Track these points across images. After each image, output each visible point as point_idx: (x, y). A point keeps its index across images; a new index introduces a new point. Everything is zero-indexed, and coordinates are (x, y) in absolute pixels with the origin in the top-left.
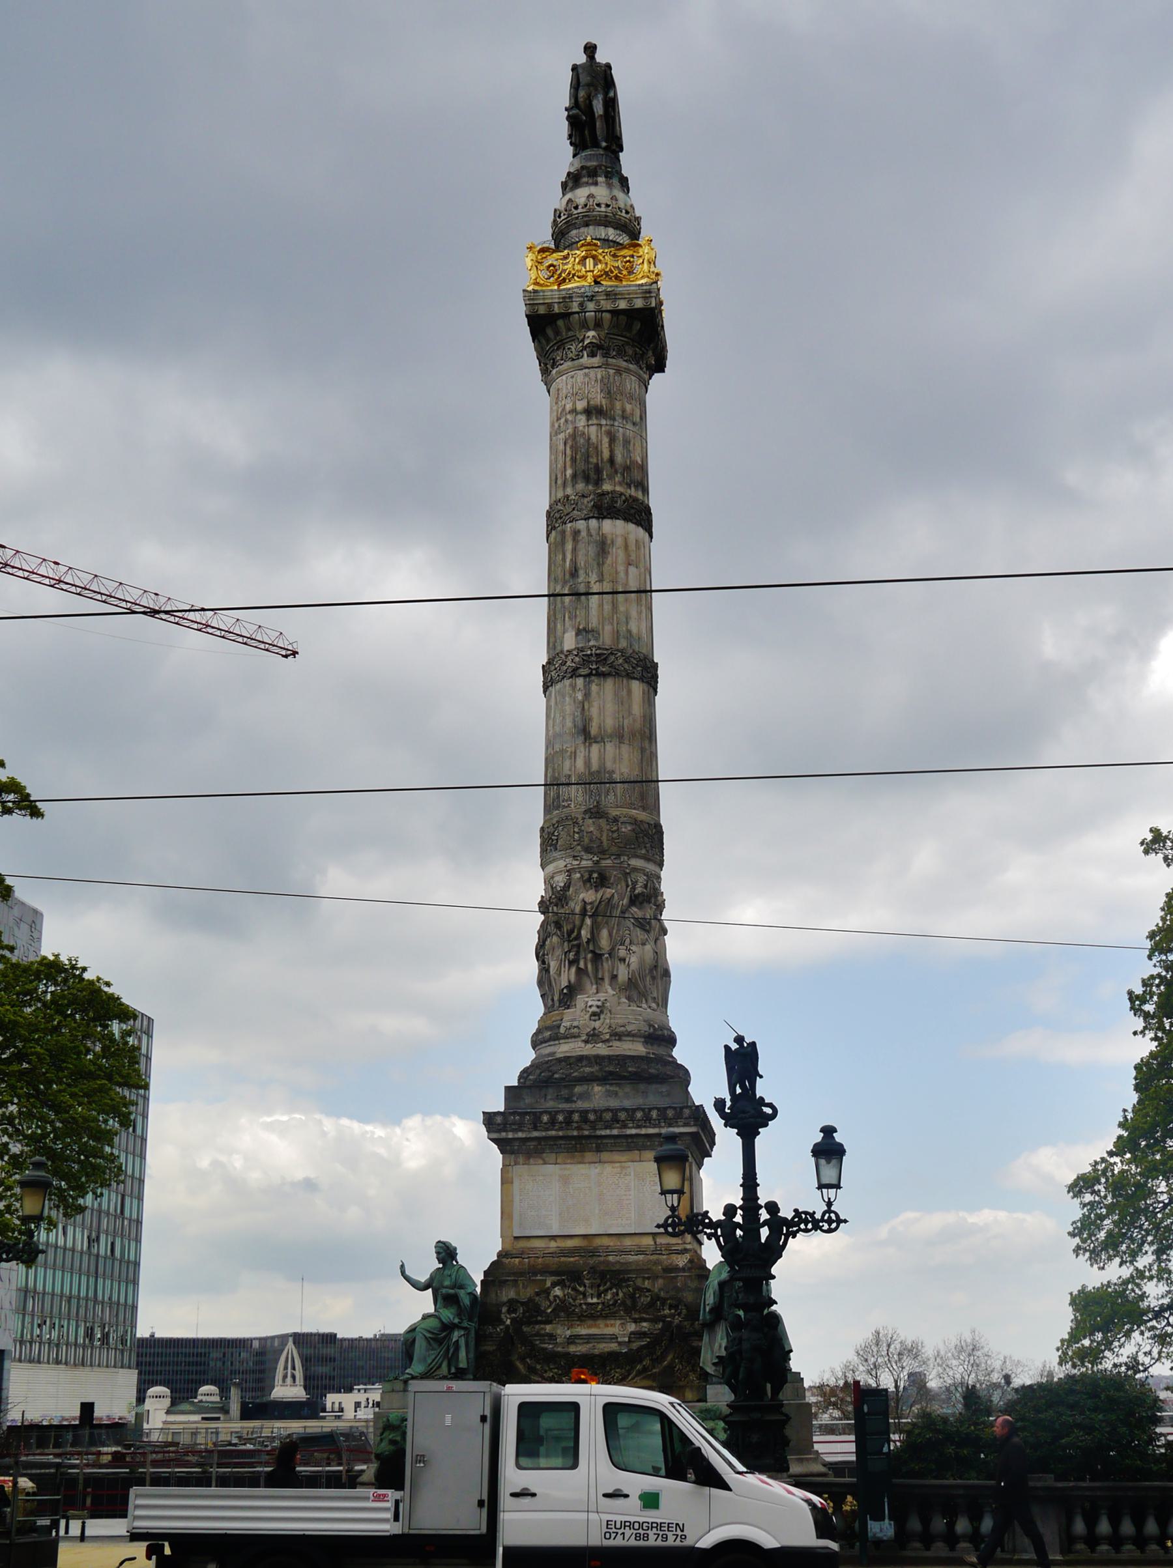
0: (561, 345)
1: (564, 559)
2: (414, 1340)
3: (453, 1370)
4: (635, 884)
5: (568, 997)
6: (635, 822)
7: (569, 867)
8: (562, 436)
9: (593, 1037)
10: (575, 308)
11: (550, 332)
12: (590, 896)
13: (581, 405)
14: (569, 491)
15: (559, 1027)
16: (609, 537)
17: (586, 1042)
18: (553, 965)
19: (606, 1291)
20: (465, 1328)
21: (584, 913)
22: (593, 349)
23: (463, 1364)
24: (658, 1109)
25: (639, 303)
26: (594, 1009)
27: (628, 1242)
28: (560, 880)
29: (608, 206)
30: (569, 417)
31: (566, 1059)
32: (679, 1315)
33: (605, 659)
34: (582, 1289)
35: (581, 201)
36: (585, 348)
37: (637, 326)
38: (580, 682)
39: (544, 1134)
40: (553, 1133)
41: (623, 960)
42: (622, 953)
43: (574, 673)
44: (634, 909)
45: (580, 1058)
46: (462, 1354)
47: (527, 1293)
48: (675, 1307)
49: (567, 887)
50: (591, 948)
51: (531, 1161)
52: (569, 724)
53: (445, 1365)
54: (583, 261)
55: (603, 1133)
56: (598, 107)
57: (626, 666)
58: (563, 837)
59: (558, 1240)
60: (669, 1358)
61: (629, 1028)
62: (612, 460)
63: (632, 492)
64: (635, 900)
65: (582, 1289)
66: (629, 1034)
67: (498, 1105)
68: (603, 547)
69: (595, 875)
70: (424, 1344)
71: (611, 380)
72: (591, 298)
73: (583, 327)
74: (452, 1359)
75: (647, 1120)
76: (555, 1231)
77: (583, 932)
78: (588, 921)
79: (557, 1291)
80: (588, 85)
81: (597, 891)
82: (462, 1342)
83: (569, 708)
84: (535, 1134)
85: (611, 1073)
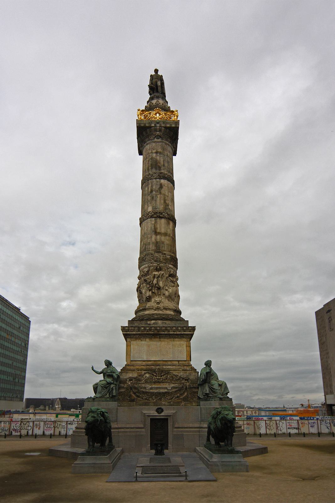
0: (148, 136)
1: (148, 188)
2: (97, 387)
3: (111, 396)
4: (170, 271)
5: (149, 299)
6: (171, 256)
7: (149, 266)
8: (148, 159)
9: (158, 309)
10: (153, 125)
11: (144, 133)
12: (156, 273)
13: (154, 151)
14: (150, 172)
15: (146, 306)
16: (163, 184)
17: (155, 310)
18: (143, 291)
19: (164, 375)
20: (115, 384)
21: (154, 277)
22: (158, 137)
23: (114, 394)
25: (173, 126)
26: (158, 301)
28: (146, 270)
29: (163, 104)
30: (151, 154)
31: (148, 314)
32: (188, 382)
33: (162, 213)
34: (155, 374)
35: (154, 103)
36: (155, 137)
38: (153, 219)
41: (167, 290)
42: (167, 288)
43: (152, 217)
44: (170, 278)
45: (154, 314)
46: (114, 391)
47: (135, 375)
48: (187, 380)
49: (148, 271)
51: (137, 340)
52: (149, 229)
53: (108, 394)
54: (156, 114)
55: (162, 333)
56: (159, 83)
60: (186, 394)
61: (169, 307)
62: (164, 165)
63: (169, 174)
64: (171, 275)
65: (155, 374)
66: (169, 309)
67: (126, 325)
68: (161, 186)
69: (158, 267)
70: (101, 388)
71: (164, 146)
72: (158, 123)
73: (155, 131)
74: (110, 392)
77: (154, 282)
78: (156, 279)
79: (147, 375)
80: (156, 78)
81: (158, 272)
82: (114, 388)
83: (150, 225)
85: (164, 318)
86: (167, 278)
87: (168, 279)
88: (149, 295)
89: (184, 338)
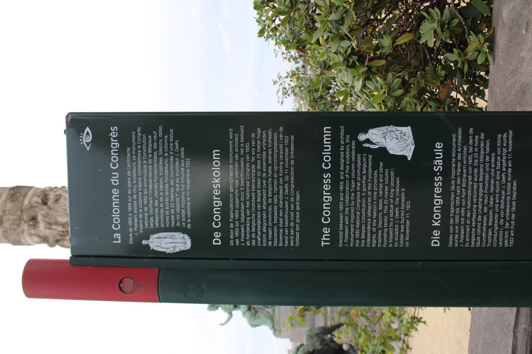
4: (37, 203)
12: (42, 225)
28: (36, 239)
44: (49, 203)
49: (39, 236)
58: (13, 237)
64: (45, 203)
87: (52, 207)
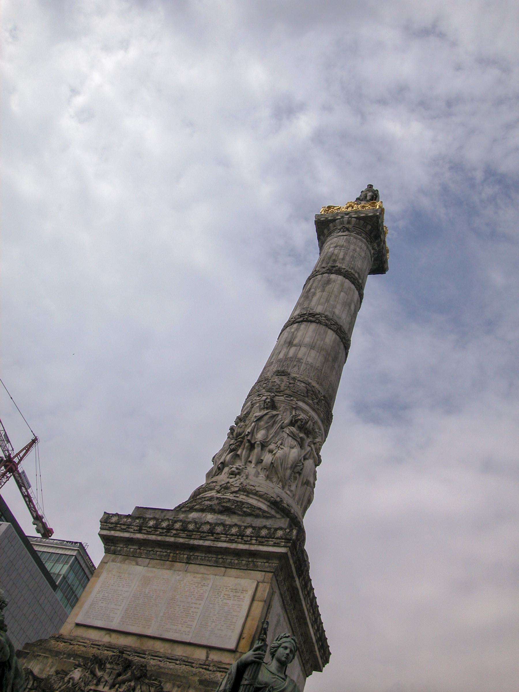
0: (330, 234)
11: (326, 231)
17: (218, 492)
24: (254, 528)
27: (179, 651)
34: (99, 674)
37: (369, 227)
39: (145, 536)
40: (153, 537)
50: (249, 438)
55: (196, 542)
57: (327, 321)
59: (114, 635)
61: (258, 489)
75: (241, 535)
76: (114, 625)
84: (139, 536)
86: (282, 428)
88: (225, 461)
89: (255, 568)
